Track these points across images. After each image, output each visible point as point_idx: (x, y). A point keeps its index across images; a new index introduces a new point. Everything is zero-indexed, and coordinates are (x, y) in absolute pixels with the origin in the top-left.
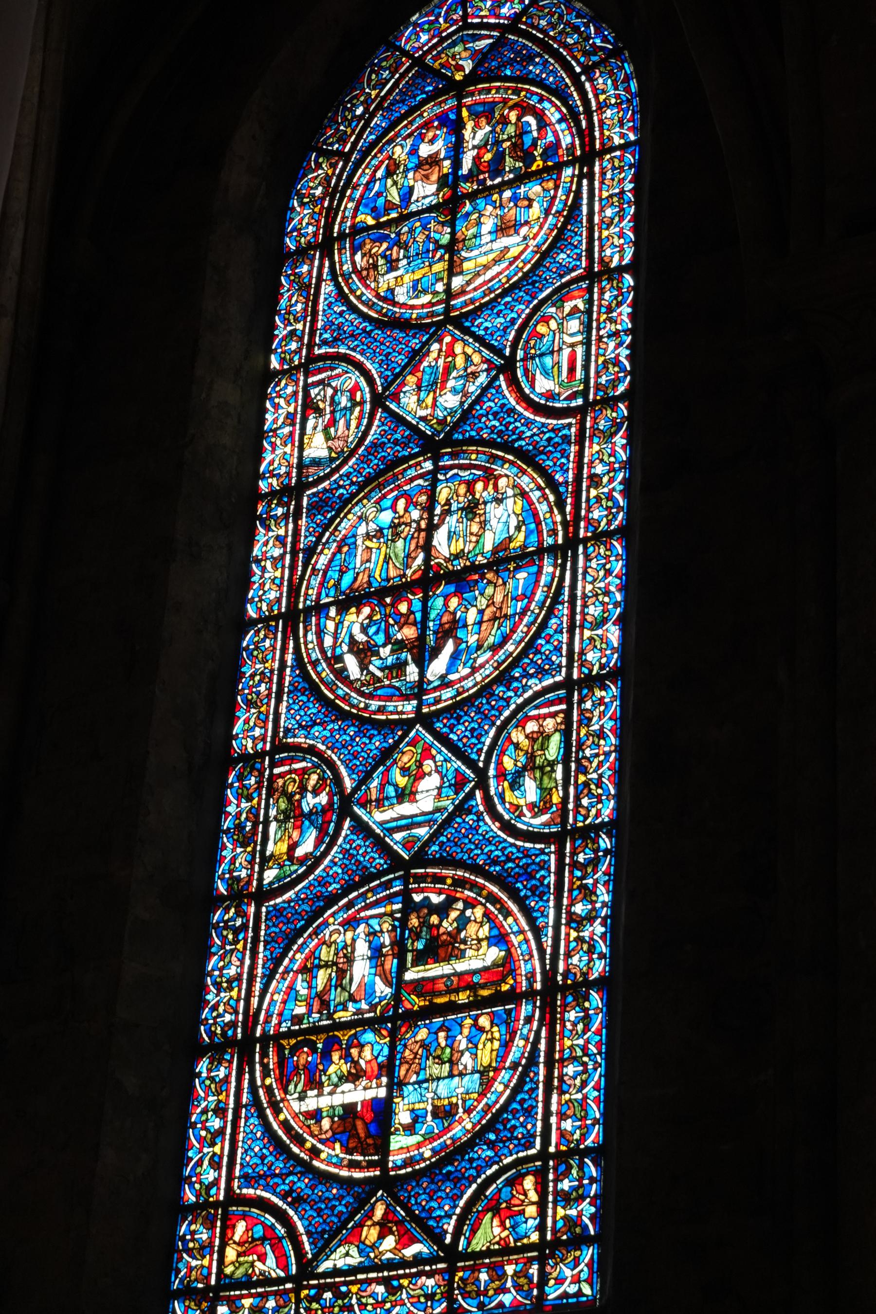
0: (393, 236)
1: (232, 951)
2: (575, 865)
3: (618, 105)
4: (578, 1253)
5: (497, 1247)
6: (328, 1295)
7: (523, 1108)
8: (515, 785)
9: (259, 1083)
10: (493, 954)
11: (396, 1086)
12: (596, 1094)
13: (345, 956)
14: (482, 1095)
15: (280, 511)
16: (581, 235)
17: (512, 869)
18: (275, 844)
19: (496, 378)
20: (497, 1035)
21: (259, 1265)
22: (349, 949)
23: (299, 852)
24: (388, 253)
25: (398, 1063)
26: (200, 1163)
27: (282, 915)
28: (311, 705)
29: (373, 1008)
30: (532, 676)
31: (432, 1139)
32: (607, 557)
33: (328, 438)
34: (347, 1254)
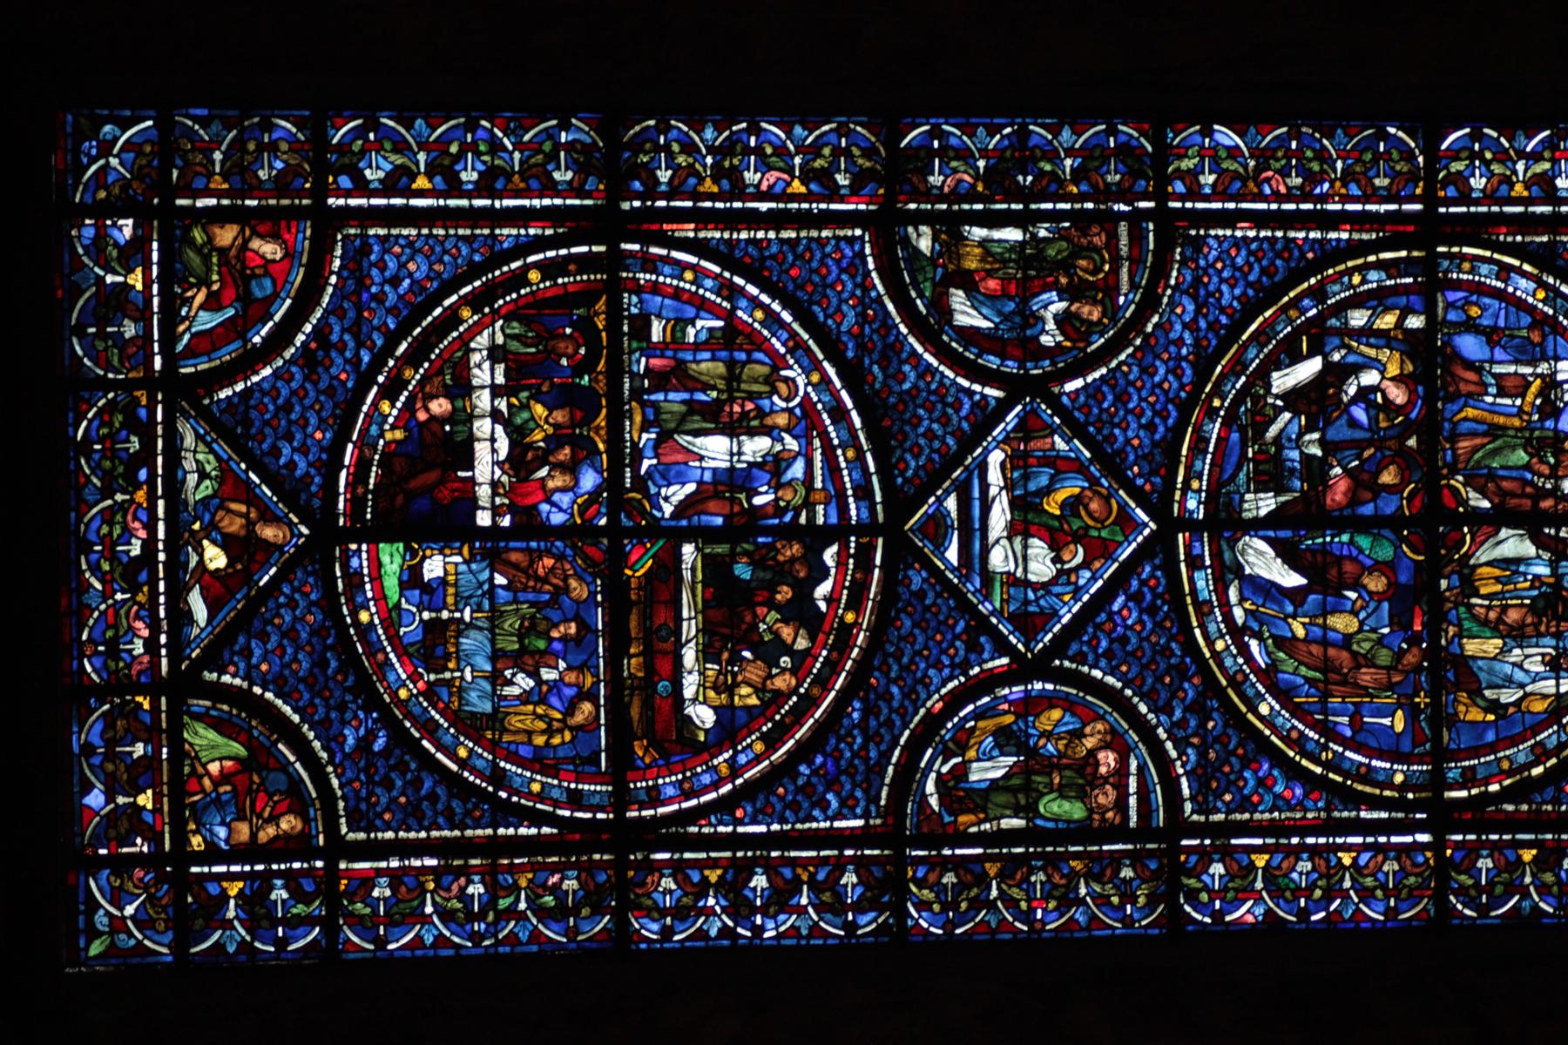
1: (789, 170)
2: (839, 866)
4: (161, 926)
5: (187, 770)
6: (135, 444)
7: (421, 800)
8: (1006, 740)
9: (531, 259)
10: (704, 716)
11: (490, 547)
12: (429, 939)
13: (744, 415)
14: (456, 718)
17: (850, 745)
18: (983, 243)
20: (556, 740)
21: (201, 297)
22: (755, 423)
23: (958, 298)
25: (534, 544)
26: (401, 147)
27: (842, 270)
28: (1237, 292)
29: (640, 483)
30: (1202, 754)
31: (391, 624)
32: (1396, 892)
34: (203, 475)
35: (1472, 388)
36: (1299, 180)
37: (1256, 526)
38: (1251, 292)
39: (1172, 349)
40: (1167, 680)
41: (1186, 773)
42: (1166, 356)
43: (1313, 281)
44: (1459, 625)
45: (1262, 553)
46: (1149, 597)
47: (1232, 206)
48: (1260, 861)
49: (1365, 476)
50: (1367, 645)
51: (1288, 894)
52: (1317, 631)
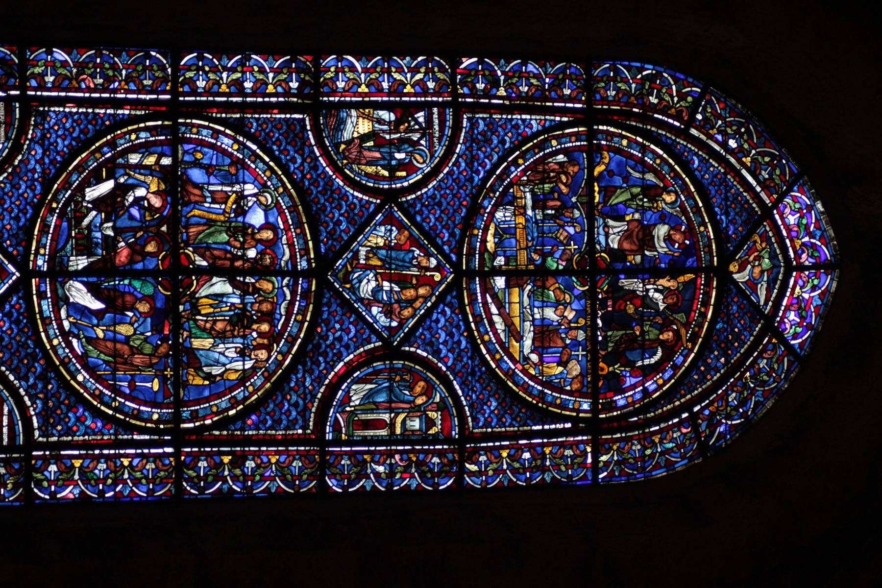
0: (574, 199)
3: (643, 456)
15: (294, 85)
16: (511, 425)
19: (380, 337)
24: (556, 195)
28: (66, 143)
32: (153, 480)
33: (364, 138)
35: (197, 198)
36: (101, 81)
37: (76, 275)
38: (74, 143)
39: (29, 174)
40: (26, 361)
41: (36, 414)
42: (26, 179)
43: (109, 137)
44: (190, 331)
45: (79, 290)
46: (15, 315)
47: (63, 94)
48: (77, 463)
49: (138, 247)
50: (138, 342)
51: (93, 482)
52: (111, 334)
